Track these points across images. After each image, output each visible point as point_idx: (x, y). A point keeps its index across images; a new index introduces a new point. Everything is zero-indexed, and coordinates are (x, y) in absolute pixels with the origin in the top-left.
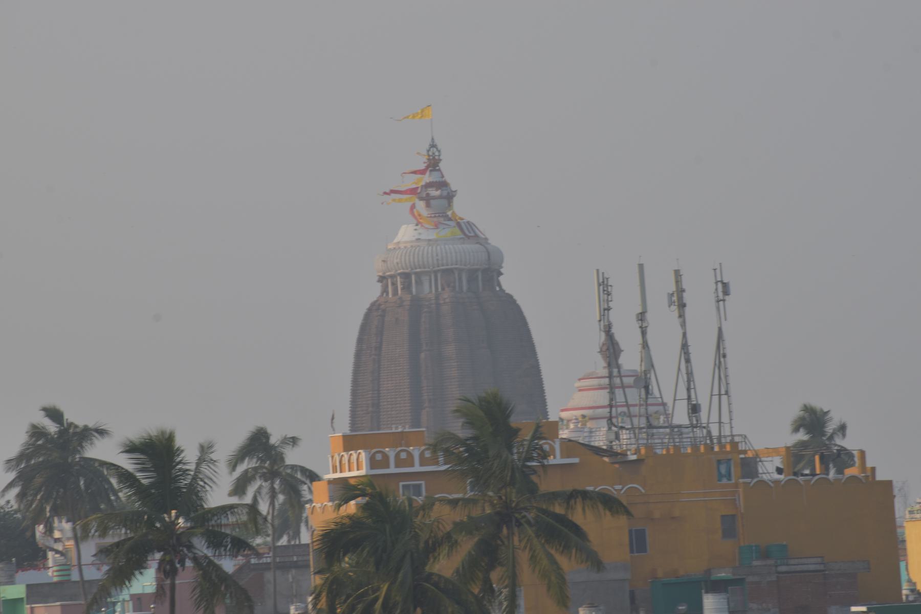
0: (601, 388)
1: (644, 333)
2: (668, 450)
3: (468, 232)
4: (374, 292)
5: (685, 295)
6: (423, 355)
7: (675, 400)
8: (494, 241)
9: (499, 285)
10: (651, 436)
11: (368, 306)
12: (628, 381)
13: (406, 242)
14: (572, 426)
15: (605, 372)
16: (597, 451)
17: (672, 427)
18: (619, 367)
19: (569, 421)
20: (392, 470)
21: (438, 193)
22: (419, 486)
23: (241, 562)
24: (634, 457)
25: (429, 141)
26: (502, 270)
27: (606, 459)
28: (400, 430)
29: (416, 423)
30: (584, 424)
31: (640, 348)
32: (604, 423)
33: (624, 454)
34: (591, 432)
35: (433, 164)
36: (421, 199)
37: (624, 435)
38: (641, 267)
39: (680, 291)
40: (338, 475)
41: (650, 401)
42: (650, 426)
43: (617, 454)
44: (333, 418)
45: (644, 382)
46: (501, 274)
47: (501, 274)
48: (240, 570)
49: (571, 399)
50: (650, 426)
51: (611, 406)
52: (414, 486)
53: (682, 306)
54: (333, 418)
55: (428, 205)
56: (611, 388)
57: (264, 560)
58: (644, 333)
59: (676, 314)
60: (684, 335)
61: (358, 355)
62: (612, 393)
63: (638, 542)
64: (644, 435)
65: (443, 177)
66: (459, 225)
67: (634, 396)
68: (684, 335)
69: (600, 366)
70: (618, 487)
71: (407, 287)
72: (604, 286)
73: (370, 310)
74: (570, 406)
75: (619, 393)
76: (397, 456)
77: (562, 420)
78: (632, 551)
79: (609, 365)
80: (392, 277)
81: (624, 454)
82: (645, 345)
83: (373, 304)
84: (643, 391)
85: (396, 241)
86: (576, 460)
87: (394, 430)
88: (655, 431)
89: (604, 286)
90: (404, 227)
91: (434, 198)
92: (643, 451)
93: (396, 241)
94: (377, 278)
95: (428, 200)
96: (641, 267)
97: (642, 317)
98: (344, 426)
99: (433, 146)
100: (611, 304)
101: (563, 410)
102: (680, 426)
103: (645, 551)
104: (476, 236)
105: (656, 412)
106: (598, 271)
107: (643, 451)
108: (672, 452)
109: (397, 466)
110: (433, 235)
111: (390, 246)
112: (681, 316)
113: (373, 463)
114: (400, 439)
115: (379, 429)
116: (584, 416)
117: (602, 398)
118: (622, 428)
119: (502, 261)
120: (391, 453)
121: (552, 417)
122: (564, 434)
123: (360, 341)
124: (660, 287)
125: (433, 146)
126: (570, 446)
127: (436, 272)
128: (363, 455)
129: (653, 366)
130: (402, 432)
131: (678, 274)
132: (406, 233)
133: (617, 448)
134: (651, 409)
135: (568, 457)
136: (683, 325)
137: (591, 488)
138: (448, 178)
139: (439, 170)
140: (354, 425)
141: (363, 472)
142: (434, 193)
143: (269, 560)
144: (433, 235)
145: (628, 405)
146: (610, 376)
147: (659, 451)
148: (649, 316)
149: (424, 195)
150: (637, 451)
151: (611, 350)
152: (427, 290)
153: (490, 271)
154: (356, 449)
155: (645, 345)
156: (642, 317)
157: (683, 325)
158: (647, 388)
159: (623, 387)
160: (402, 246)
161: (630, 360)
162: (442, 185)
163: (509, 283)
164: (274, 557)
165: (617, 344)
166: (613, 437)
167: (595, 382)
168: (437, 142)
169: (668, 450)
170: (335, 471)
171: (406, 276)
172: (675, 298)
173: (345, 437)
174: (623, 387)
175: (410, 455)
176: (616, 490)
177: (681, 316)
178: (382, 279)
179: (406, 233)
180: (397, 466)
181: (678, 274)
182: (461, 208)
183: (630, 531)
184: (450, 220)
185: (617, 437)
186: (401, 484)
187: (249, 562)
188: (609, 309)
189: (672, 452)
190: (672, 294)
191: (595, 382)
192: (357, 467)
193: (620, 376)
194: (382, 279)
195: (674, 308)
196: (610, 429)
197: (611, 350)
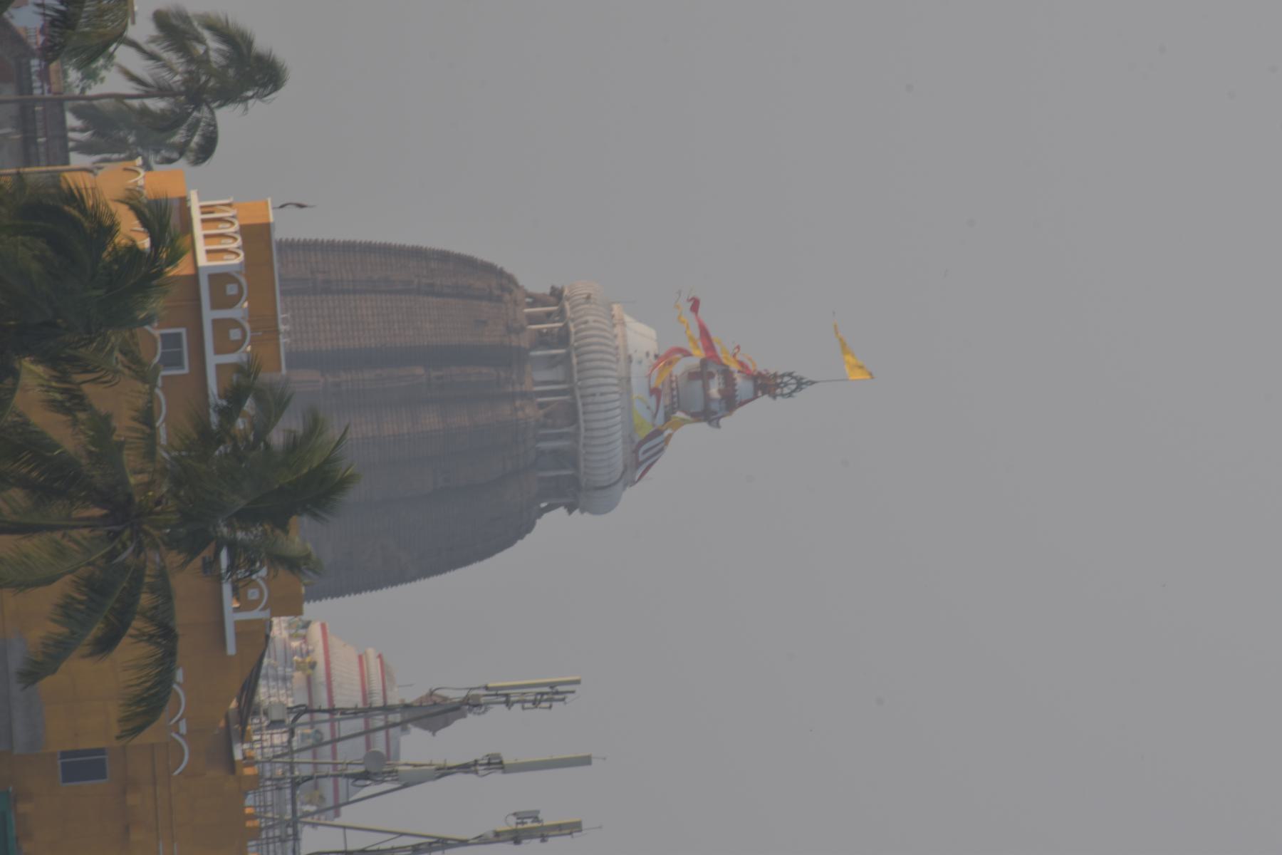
0: (366, 694)
1: (466, 768)
2: (252, 817)
3: (644, 452)
4: (534, 281)
5: (536, 841)
6: (419, 371)
7: (344, 827)
8: (630, 497)
9: (550, 508)
10: (278, 784)
11: (509, 269)
12: (379, 741)
13: (624, 336)
14: (295, 644)
15: (394, 700)
16: (250, 687)
17: (294, 823)
18: (403, 725)
19: (304, 638)
20: (209, 315)
21: (714, 391)
22: (179, 364)
23: (32, 41)
24: (238, 755)
25: (808, 376)
26: (577, 512)
27: (234, 704)
28: (282, 328)
29: (297, 360)
30: (298, 667)
31: (439, 761)
32: (302, 699)
33: (243, 736)
34: (285, 679)
35: (766, 385)
36: (704, 363)
37: (279, 738)
38: (586, 761)
39: (543, 834)
40: (196, 216)
41: (342, 782)
42: (296, 783)
43: (243, 723)
44: (301, 206)
45: (377, 771)
46: (571, 509)
47: (571, 509)
48: (17, 39)
49: (343, 643)
50: (296, 783)
51: (332, 711)
52: (180, 355)
53: (516, 837)
54: (301, 206)
55: (693, 376)
56: (365, 711)
57: (37, 84)
58: (466, 768)
59: (502, 827)
60: (464, 843)
61: (418, 254)
62: (356, 712)
63: (83, 766)
64: (279, 772)
65: (742, 403)
66: (658, 432)
67: (352, 752)
68: (464, 843)
69: (407, 692)
70: (183, 728)
71: (543, 340)
72: (550, 695)
73: (500, 273)
74: (333, 640)
75: (358, 724)
76: (234, 323)
77: (306, 625)
78: (65, 754)
79: (406, 707)
80: (562, 312)
81: (243, 736)
82: (444, 771)
83: (510, 279)
84: (360, 769)
85: (627, 319)
86: (231, 649)
87: (281, 316)
88: (288, 792)
89: (550, 695)
90: (651, 332)
91: (706, 388)
92: (248, 771)
93: (627, 319)
94: (558, 285)
95: (700, 375)
96: (586, 761)
97: (495, 764)
98: (287, 228)
99: (801, 384)
100: (517, 707)
101: (323, 627)
102: (296, 837)
103: (65, 780)
104: (638, 464)
105: (322, 798)
106: (577, 682)
107: (248, 771)
108: (249, 824)
109: (216, 322)
110: (639, 388)
111: (616, 309)
112: (498, 837)
113: (220, 279)
114: (265, 326)
115: (282, 293)
116: (313, 665)
117: (348, 696)
118: (292, 733)
119: (595, 512)
120: (240, 311)
121: (311, 609)
122: (280, 628)
123: (444, 257)
124: (550, 797)
125: (801, 384)
126: (257, 638)
127: (570, 392)
128: (235, 261)
129: (405, 786)
130: (277, 332)
131: (574, 827)
132: (641, 338)
133: (254, 723)
134: (327, 785)
135: (238, 635)
136: (482, 840)
137: (179, 675)
138: (739, 412)
139: (756, 397)
140: (290, 247)
141: (202, 260)
142: (712, 388)
143: (37, 92)
144: (639, 388)
145: (334, 741)
146: (387, 709)
147: (249, 800)
148: (497, 777)
149: (712, 368)
150: (249, 761)
151: (435, 713)
152: (539, 377)
153: (575, 489)
154: (245, 247)
155: (444, 771)
156: (495, 764)
157: (482, 840)
158: (366, 776)
159: (368, 732)
160: (618, 330)
161: (416, 746)
162: (731, 402)
163: (555, 525)
164: (43, 101)
165: (446, 724)
166: (275, 715)
167: (376, 685)
168: (808, 390)
169: (252, 817)
170: (205, 210)
171: (563, 338)
172: (529, 824)
173: (266, 228)
174: (368, 732)
175: (238, 345)
176: (177, 723)
177: (498, 837)
178: (557, 295)
179: (641, 338)
180: (216, 322)
181: (574, 827)
182: (689, 438)
183: (101, 751)
184: (667, 418)
185: (275, 724)
186: (183, 331)
187: (33, 55)
188: (508, 703)
189: (249, 824)
190: (536, 819)
191: (376, 685)
192: (210, 251)
193: (387, 727)
194: (557, 295)
195: (512, 823)
196: (290, 710)
197: (435, 713)
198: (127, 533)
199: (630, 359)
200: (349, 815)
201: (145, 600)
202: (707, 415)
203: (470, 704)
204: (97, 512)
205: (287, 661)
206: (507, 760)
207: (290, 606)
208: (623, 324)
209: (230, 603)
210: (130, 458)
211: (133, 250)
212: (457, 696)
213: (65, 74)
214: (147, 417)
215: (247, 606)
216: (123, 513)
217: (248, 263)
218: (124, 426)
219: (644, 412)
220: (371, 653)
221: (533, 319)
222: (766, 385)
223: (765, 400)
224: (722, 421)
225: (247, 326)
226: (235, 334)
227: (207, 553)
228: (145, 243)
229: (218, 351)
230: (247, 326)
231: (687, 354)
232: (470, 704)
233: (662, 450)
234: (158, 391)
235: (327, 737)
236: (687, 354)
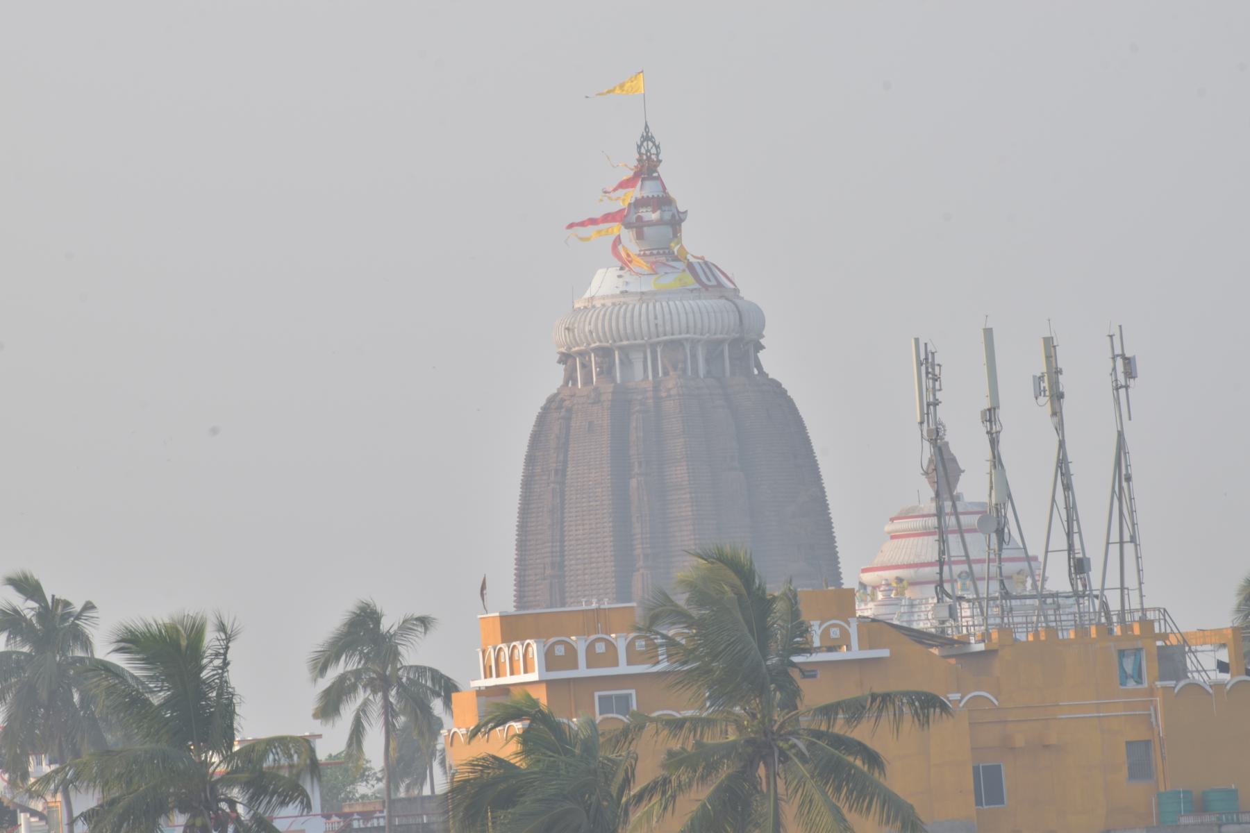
1: (994, 443)
2: (1036, 634)
3: (707, 279)
4: (553, 379)
7: (1047, 552)
8: (749, 293)
9: (759, 366)
10: (1006, 612)
11: (543, 402)
12: (969, 521)
13: (603, 297)
14: (880, 596)
15: (931, 507)
16: (920, 637)
17: (1043, 597)
18: (954, 499)
19: (875, 588)
20: (583, 671)
21: (654, 216)
22: (627, 698)
23: (336, 827)
24: (981, 647)
25: (640, 130)
26: (762, 341)
27: (935, 651)
28: (594, 606)
29: (623, 593)
30: (900, 593)
32: (931, 589)
33: (964, 642)
35: (647, 169)
36: (628, 226)
37: (965, 610)
38: (988, 333)
39: (1054, 372)
41: (1005, 554)
42: (1006, 595)
43: (952, 642)
44: (483, 587)
45: (996, 522)
49: (878, 552)
50: (1006, 595)
51: (941, 563)
52: (618, 697)
53: (1057, 396)
54: (483, 587)
55: (640, 236)
56: (941, 534)
57: (375, 823)
58: (994, 443)
59: (1048, 409)
60: (1062, 444)
61: (528, 483)
62: (943, 541)
64: (996, 610)
65: (664, 188)
67: (978, 545)
68: (1062, 444)
70: (957, 696)
71: (607, 372)
72: (928, 366)
73: (546, 410)
74: (877, 562)
75: (953, 540)
76: (590, 648)
77: (863, 586)
78: (978, 802)
79: (938, 495)
80: (581, 354)
81: (964, 642)
82: (996, 461)
83: (551, 400)
84: (994, 537)
85: (587, 295)
86: (885, 653)
87: (584, 607)
88: (1014, 602)
89: (928, 366)
90: (600, 273)
91: (651, 224)
92: (995, 636)
94: (558, 356)
95: (639, 227)
96: (988, 333)
97: (990, 415)
98: (504, 599)
99: (647, 137)
100: (939, 395)
101: (864, 571)
102: (1055, 595)
104: (720, 285)
106: (917, 340)
107: (995, 636)
108: (1043, 638)
109: (589, 665)
110: (648, 285)
111: (579, 304)
112: (1056, 413)
113: (550, 661)
114: (594, 621)
115: (563, 605)
116: (899, 580)
117: (927, 549)
118: (961, 598)
121: (848, 582)
122: (866, 609)
123: (530, 460)
125: (647, 137)
126: (874, 629)
127: (653, 347)
129: (1010, 496)
130: (598, 610)
131: (1049, 344)
132: (605, 282)
134: (1008, 568)
135: (871, 648)
136: (1060, 428)
138: (672, 192)
139: (659, 178)
141: (533, 676)
142: (651, 218)
143: (382, 822)
145: (968, 561)
146: (940, 514)
147: (1021, 637)
148: (1002, 414)
149: (633, 218)
150: (985, 637)
151: (943, 470)
153: (743, 343)
155: (996, 461)
156: (990, 415)
157: (1060, 428)
158: (1000, 532)
159: (961, 531)
160: (598, 304)
161: (974, 487)
162: (663, 201)
164: (390, 818)
165: (954, 460)
166: (945, 613)
167: (917, 523)
168: (653, 131)
170: (488, 674)
171: (605, 353)
172: (1045, 384)
173: (504, 619)
174: (961, 531)
175: (611, 646)
178: (565, 358)
179: (605, 282)
180: (589, 665)
181: (1049, 344)
182: (695, 240)
183: (976, 770)
184: (676, 259)
185: (952, 614)
186: (597, 694)
187: (349, 825)
188: (936, 403)
189: (1043, 638)
190: (1041, 378)
191: (917, 523)
192: (526, 671)
193: (956, 513)
195: (1044, 400)
197: (943, 470)
198: (781, 744)
199: (624, 293)
200: (1036, 549)
201: (840, 727)
202: (675, 222)
203: (935, 436)
204: (762, 771)
205: (896, 603)
206: (986, 404)
207: (845, 601)
208: (592, 298)
209: (843, 654)
210: (711, 738)
211: (525, 738)
212: (928, 450)
213: (363, 797)
214: (676, 725)
215: (845, 638)
216: (762, 748)
217: (536, 636)
218: (682, 743)
219: (669, 280)
220: (889, 527)
221: (588, 380)
222: (647, 169)
223: (661, 170)
224: (681, 209)
225: (593, 637)
226: (600, 648)
227: (795, 674)
228: (517, 726)
229: (616, 664)
230: (593, 637)
231: (617, 241)
232: (935, 436)
233: (706, 263)
234: (655, 714)
235: (965, 567)
236: (617, 241)
